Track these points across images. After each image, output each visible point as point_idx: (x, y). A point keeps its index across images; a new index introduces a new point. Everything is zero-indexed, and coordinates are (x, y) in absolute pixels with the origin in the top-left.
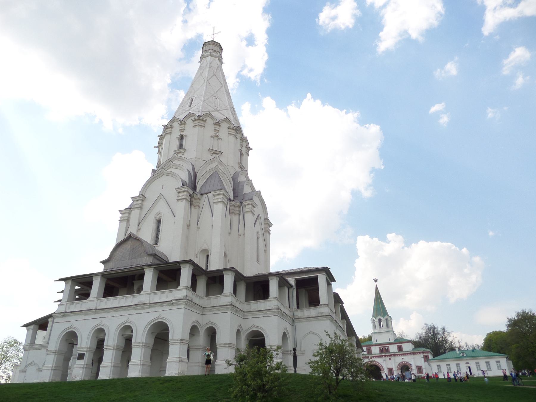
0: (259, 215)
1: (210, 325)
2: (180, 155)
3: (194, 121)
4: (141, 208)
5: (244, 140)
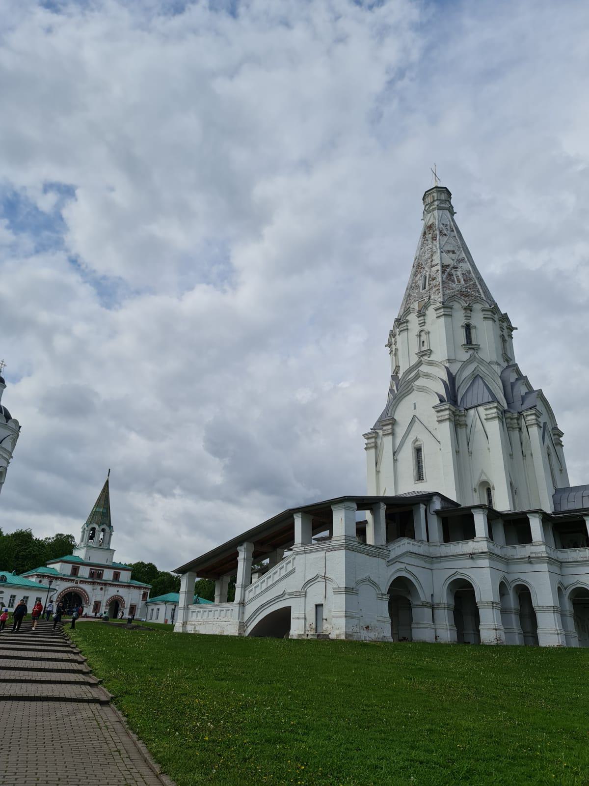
0: (545, 423)
2: (426, 357)
3: (436, 310)
4: (393, 434)
5: (505, 318)
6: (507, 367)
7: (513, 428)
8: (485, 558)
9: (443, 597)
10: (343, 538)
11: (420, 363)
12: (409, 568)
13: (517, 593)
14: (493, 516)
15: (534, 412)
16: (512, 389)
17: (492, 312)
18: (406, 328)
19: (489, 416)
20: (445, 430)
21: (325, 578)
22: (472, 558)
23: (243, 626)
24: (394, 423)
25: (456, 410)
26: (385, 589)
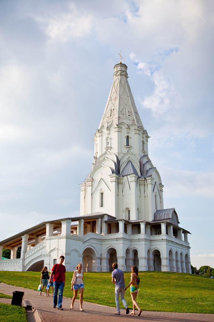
0: (156, 182)
1: (135, 249)
4: (92, 186)
5: (145, 132)
6: (144, 156)
7: (142, 185)
8: (121, 240)
9: (105, 255)
10: (66, 234)
11: (106, 153)
12: (92, 244)
13: (134, 252)
14: (127, 223)
15: (150, 178)
16: (143, 167)
17: (139, 130)
18: (101, 135)
19: (132, 180)
20: (113, 186)
21: (58, 249)
22: (117, 240)
23: (24, 267)
24: (93, 180)
25: (119, 176)
26: (81, 252)
